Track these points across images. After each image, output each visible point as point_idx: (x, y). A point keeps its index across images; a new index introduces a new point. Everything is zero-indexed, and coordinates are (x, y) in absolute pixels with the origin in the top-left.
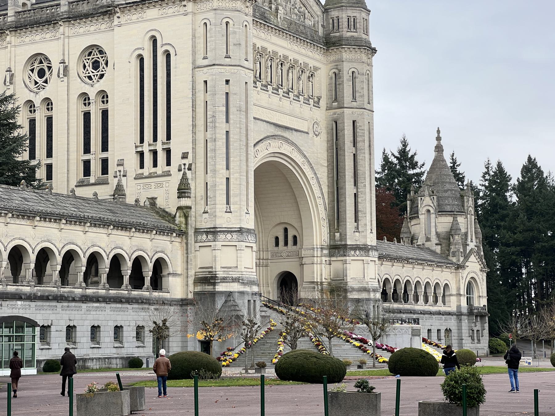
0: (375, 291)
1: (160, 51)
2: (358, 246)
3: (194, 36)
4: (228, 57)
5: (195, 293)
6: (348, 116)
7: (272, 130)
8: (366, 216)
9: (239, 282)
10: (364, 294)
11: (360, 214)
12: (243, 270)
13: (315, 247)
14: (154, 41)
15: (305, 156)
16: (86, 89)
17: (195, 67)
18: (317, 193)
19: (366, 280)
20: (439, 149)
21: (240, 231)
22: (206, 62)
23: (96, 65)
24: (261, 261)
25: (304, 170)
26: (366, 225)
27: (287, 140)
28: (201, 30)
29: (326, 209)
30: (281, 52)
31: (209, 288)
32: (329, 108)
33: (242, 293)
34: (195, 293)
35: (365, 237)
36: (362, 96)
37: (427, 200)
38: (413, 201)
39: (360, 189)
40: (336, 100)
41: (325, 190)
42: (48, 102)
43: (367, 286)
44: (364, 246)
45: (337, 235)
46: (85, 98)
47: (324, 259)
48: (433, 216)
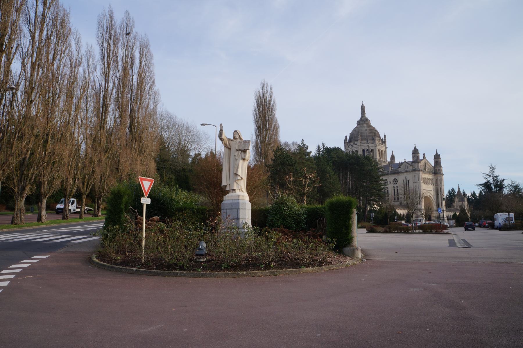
0: (445, 218)
1: (407, 180)
3: (413, 178)
4: (419, 181)
5: (415, 219)
6: (439, 187)
7: (426, 191)
14: (406, 178)
16: (394, 186)
17: (413, 183)
18: (434, 201)
20: (459, 188)
21: (422, 209)
22: (415, 182)
23: (396, 182)
28: (414, 177)
30: (427, 177)
31: (417, 218)
32: (436, 185)
34: (415, 219)
36: (442, 183)
37: (457, 199)
38: (454, 199)
40: (437, 184)
41: (436, 200)
42: (388, 188)
46: (394, 187)
48: (458, 202)
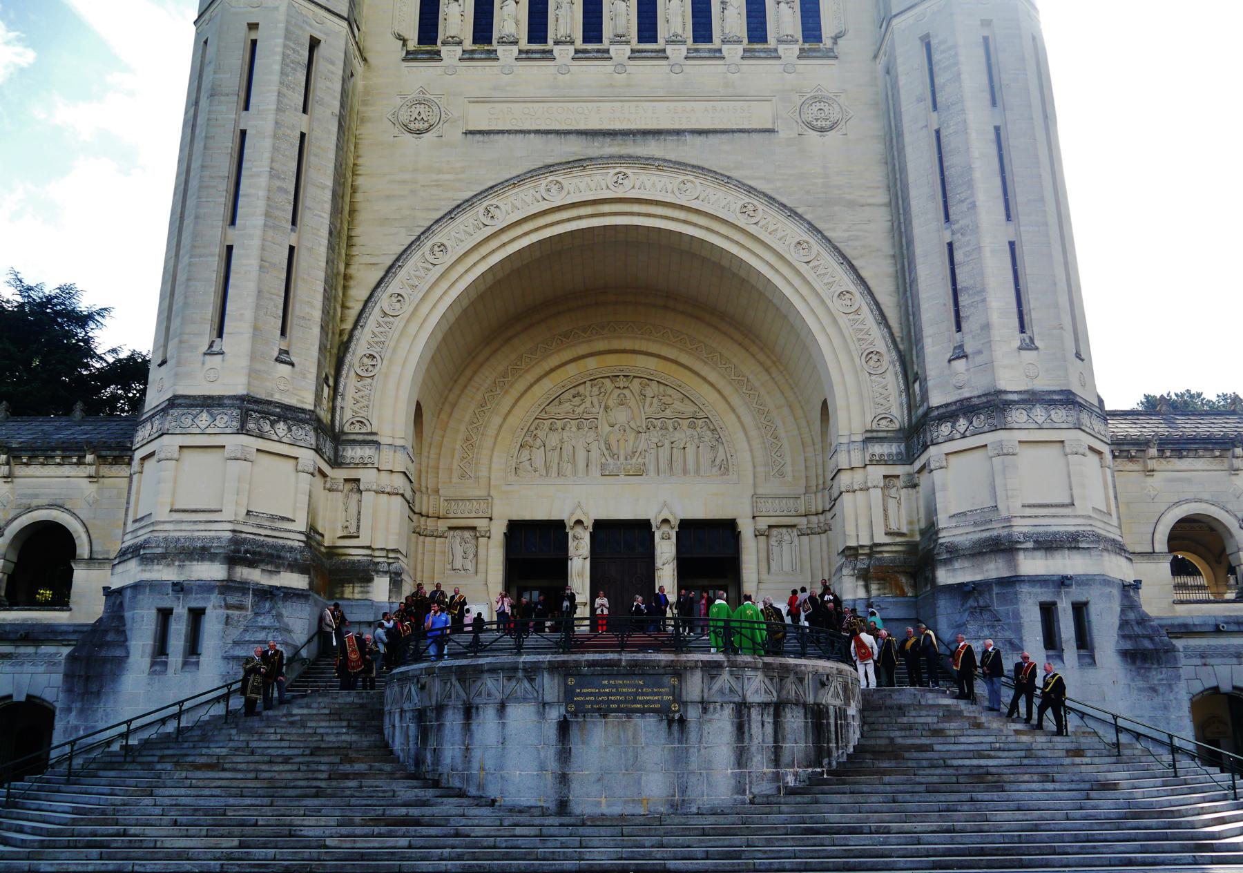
2: (965, 403)
8: (984, 300)
9: (139, 555)
10: (992, 566)
11: (964, 300)
12: (162, 514)
13: (844, 440)
15: (751, 190)
19: (1004, 513)
24: (814, 519)
25: (752, 229)
26: (986, 327)
27: (648, 162)
29: (883, 319)
33: (137, 587)
35: (989, 366)
39: (957, 221)
43: (1004, 532)
44: (984, 399)
45: (917, 385)
47: (877, 473)
